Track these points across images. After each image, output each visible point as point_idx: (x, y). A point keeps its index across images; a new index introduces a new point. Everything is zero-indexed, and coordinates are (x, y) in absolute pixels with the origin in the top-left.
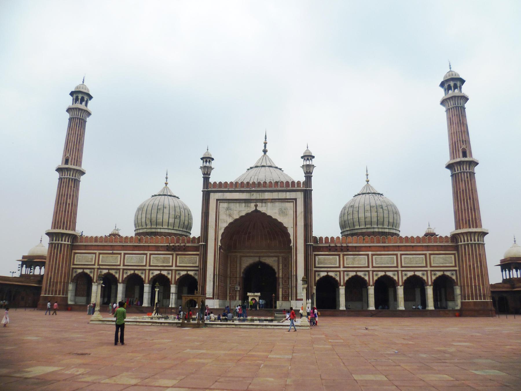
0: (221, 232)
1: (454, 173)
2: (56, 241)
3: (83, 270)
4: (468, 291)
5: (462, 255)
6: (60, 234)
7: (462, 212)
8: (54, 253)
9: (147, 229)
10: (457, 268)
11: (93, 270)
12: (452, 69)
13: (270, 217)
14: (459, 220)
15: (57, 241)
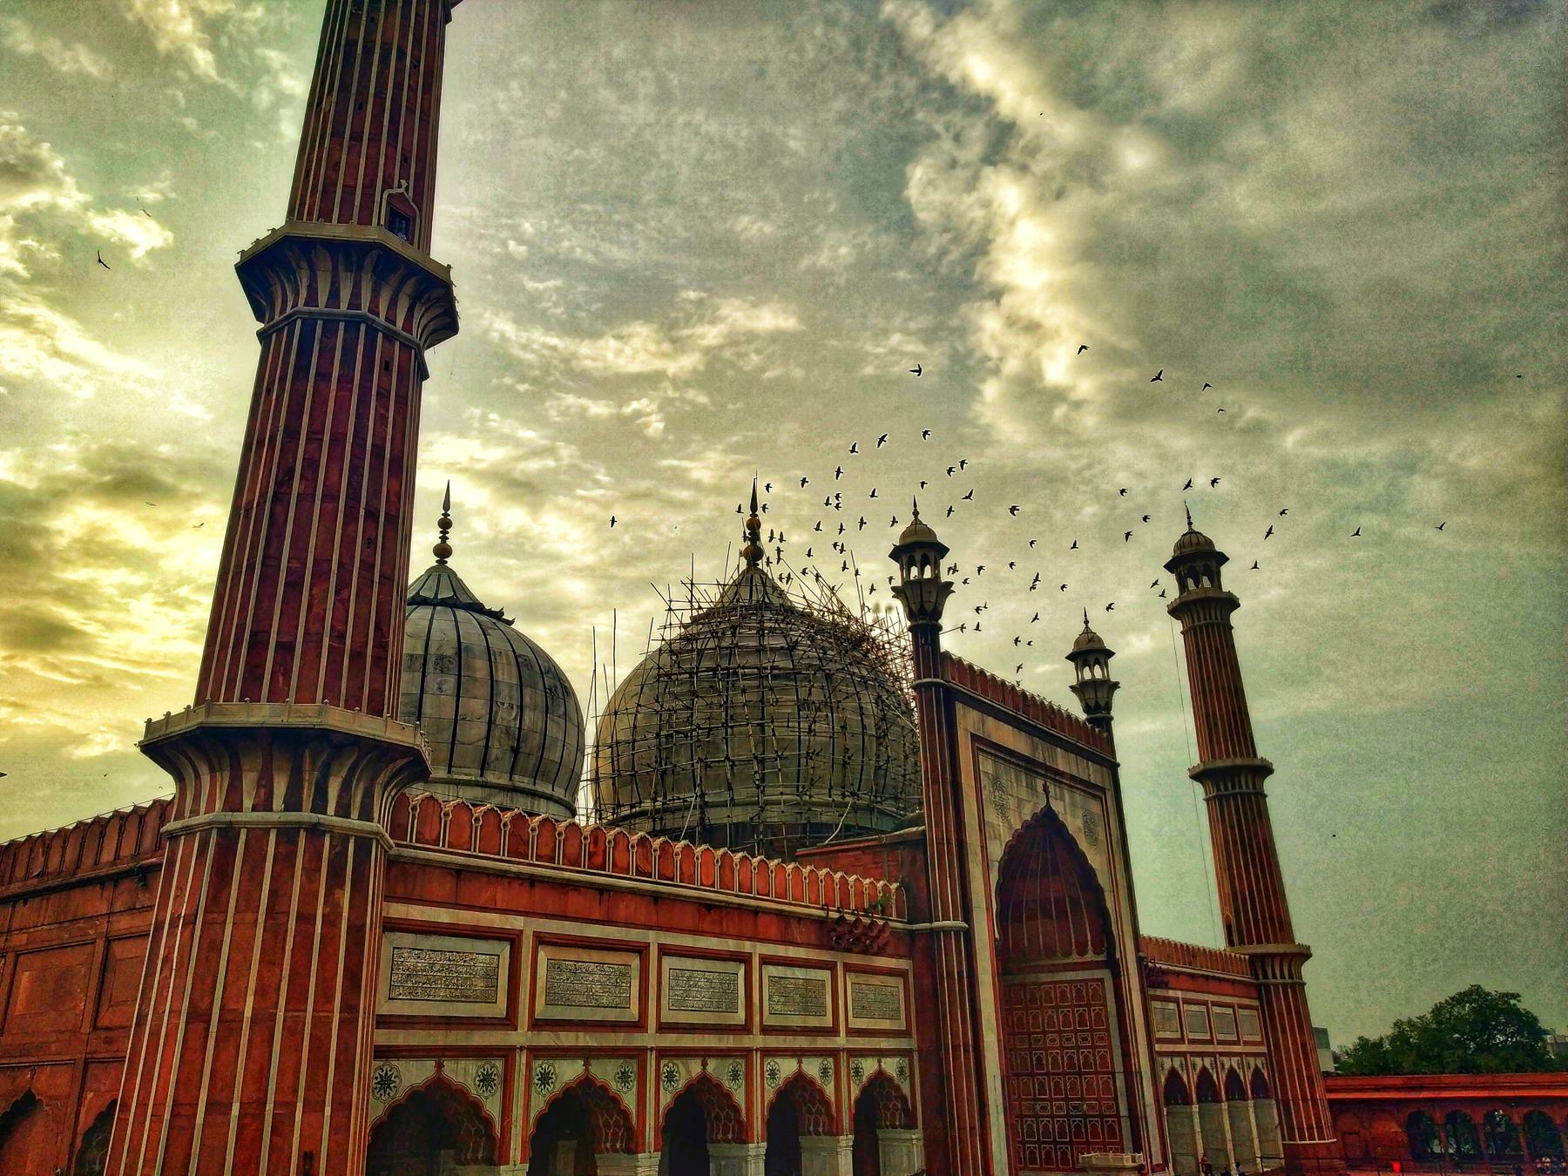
0: (994, 877)
1: (1237, 790)
2: (343, 810)
3: (439, 1066)
4: (1308, 1118)
5: (1281, 1014)
6: (401, 762)
7: (1268, 897)
8: (331, 921)
9: (487, 790)
10: (1264, 1049)
11: (499, 1064)
12: (1196, 527)
13: (1071, 843)
14: (1263, 917)
15: (355, 814)
